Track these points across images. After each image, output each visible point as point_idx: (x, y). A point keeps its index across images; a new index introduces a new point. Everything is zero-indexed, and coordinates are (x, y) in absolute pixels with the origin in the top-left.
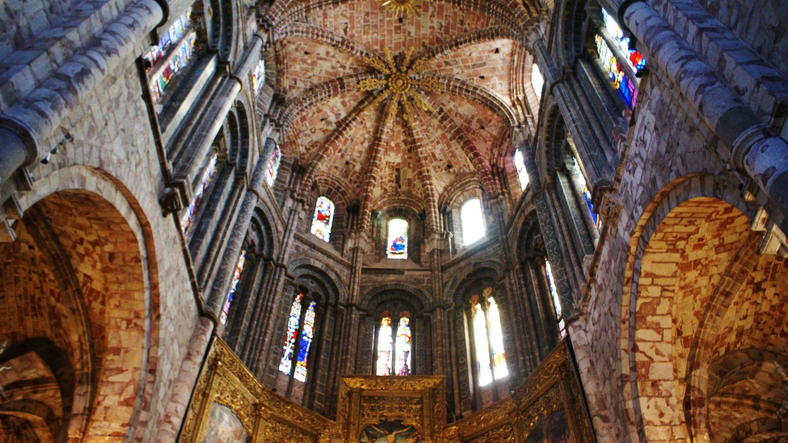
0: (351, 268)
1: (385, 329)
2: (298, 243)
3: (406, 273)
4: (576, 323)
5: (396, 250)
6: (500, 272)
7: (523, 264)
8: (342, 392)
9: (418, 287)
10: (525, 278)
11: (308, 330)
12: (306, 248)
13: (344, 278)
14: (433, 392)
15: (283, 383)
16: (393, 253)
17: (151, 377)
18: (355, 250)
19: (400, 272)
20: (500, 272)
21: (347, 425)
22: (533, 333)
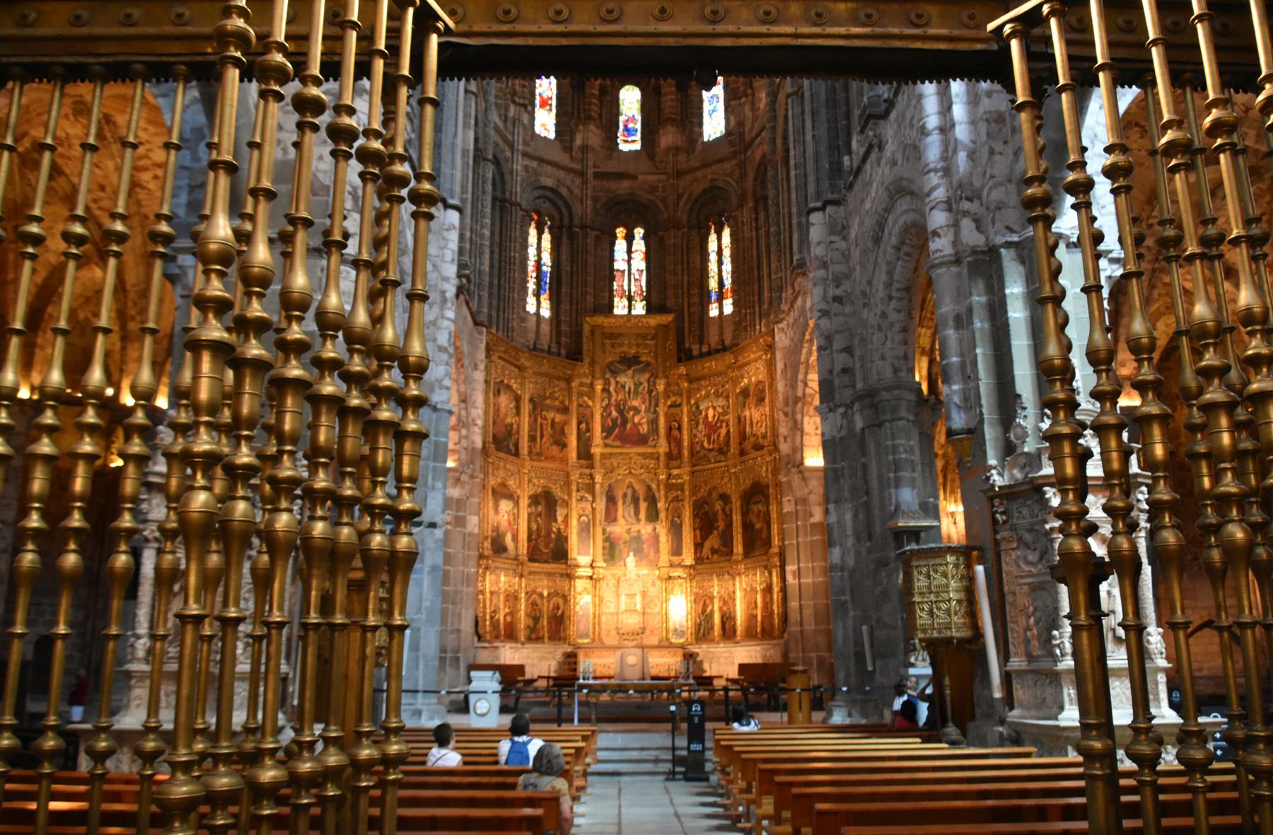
0: (582, 174)
1: (620, 246)
2: (527, 162)
3: (640, 177)
4: (781, 326)
5: (629, 135)
6: (734, 200)
7: (756, 202)
8: (586, 328)
9: (652, 197)
10: (757, 220)
11: (546, 258)
12: (534, 164)
13: (577, 191)
14: (665, 327)
15: (532, 323)
16: (626, 141)
17: (463, 405)
18: (585, 148)
19: (634, 177)
20: (734, 200)
21: (592, 364)
22: (756, 287)
